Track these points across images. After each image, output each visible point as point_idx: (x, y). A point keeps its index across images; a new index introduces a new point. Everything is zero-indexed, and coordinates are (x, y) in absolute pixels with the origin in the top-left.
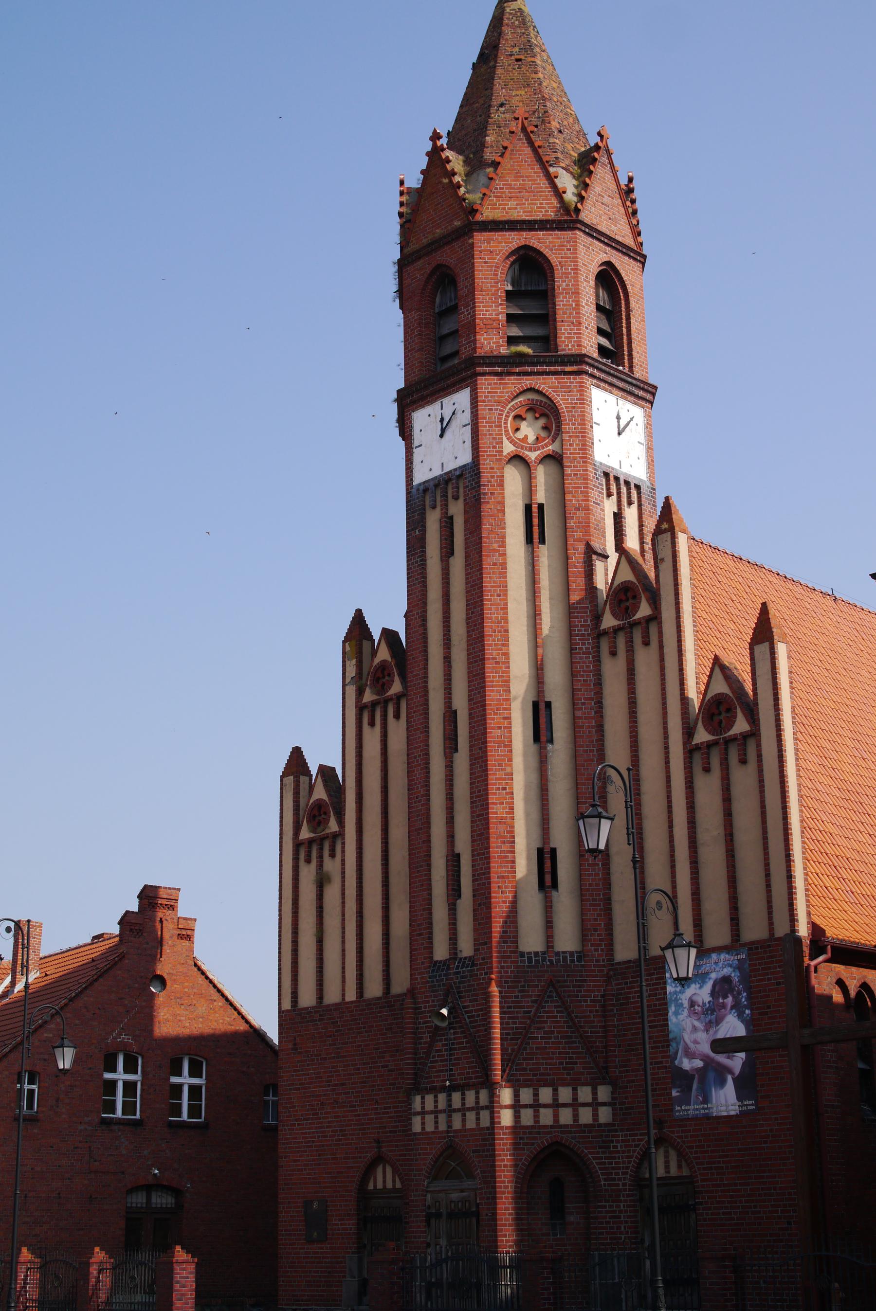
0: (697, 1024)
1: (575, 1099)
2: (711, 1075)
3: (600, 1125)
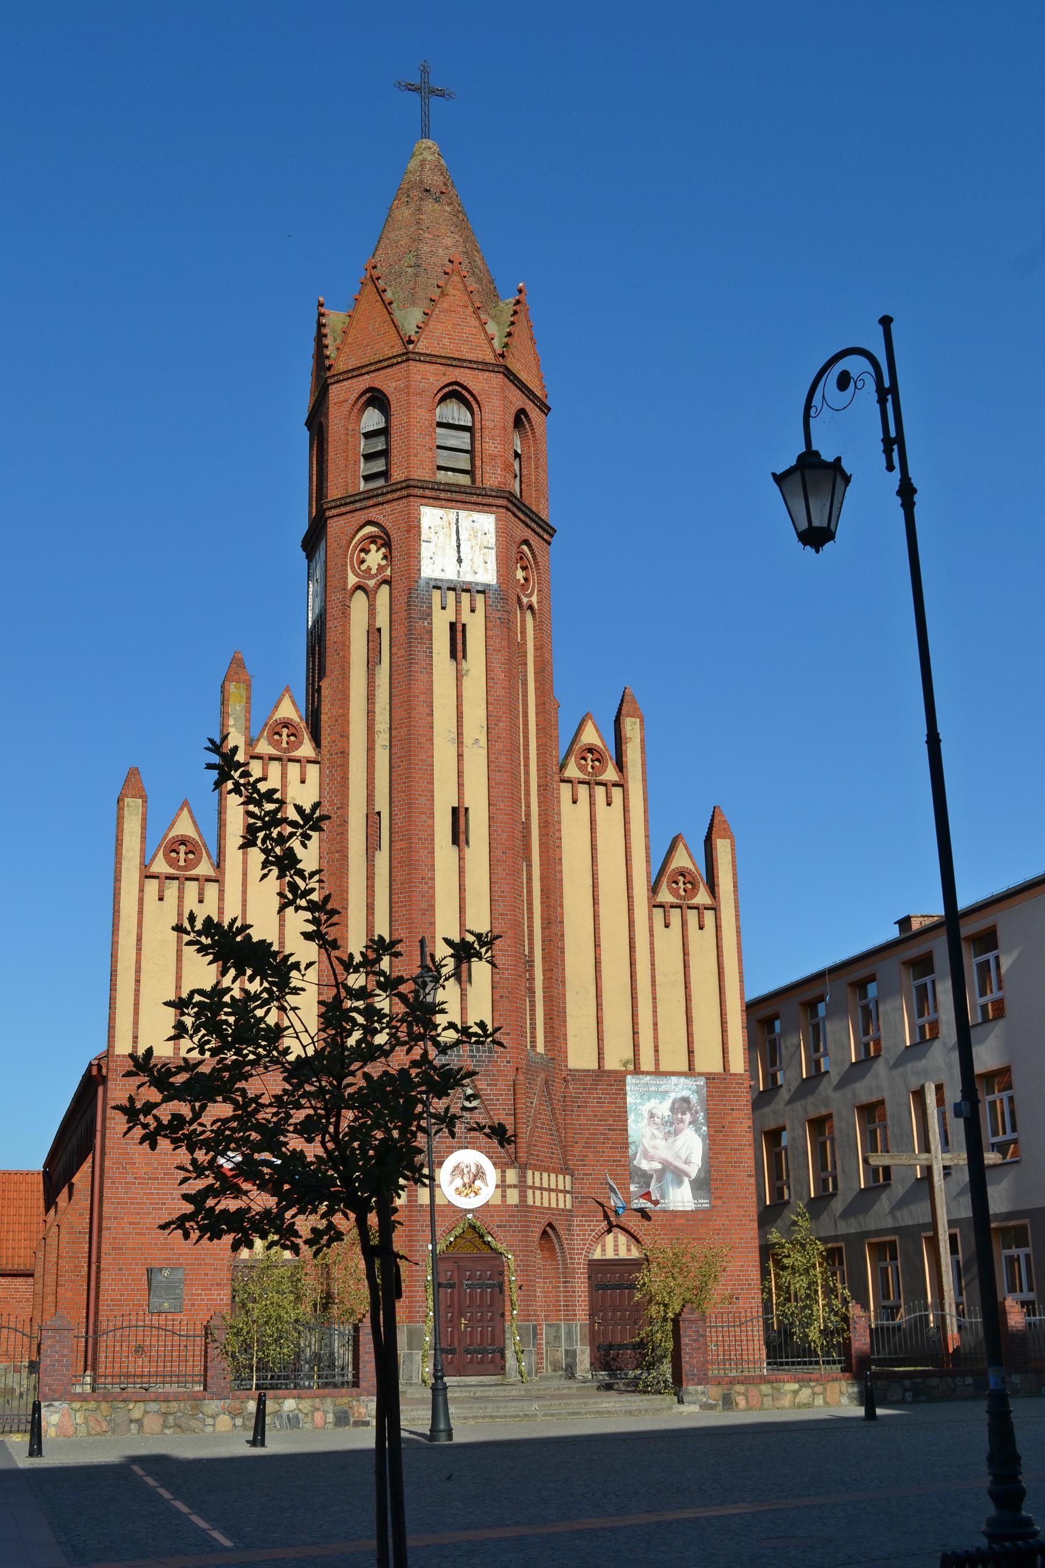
0: (656, 1132)
2: (669, 1176)
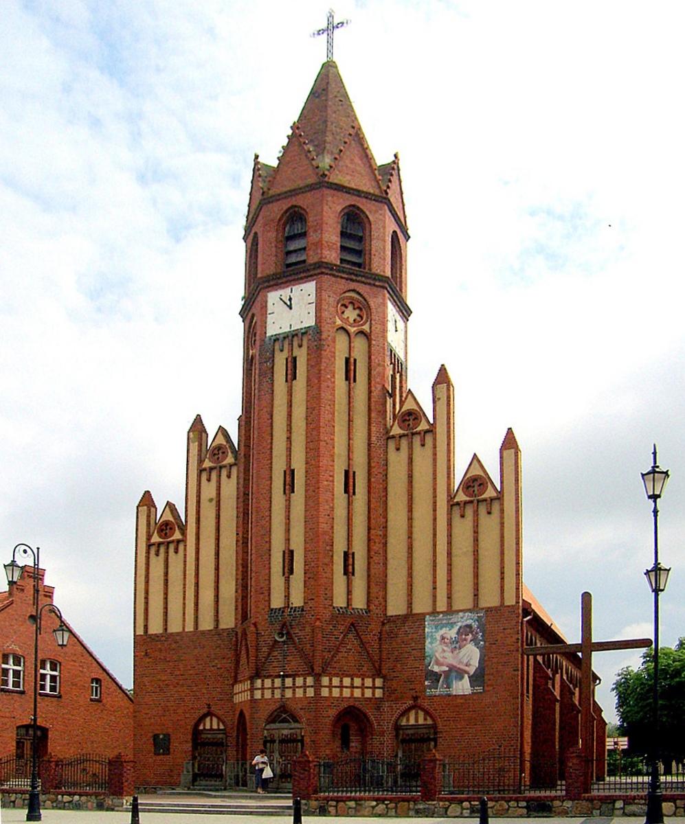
0: (445, 648)
1: (363, 684)
2: (454, 674)
3: (376, 698)
